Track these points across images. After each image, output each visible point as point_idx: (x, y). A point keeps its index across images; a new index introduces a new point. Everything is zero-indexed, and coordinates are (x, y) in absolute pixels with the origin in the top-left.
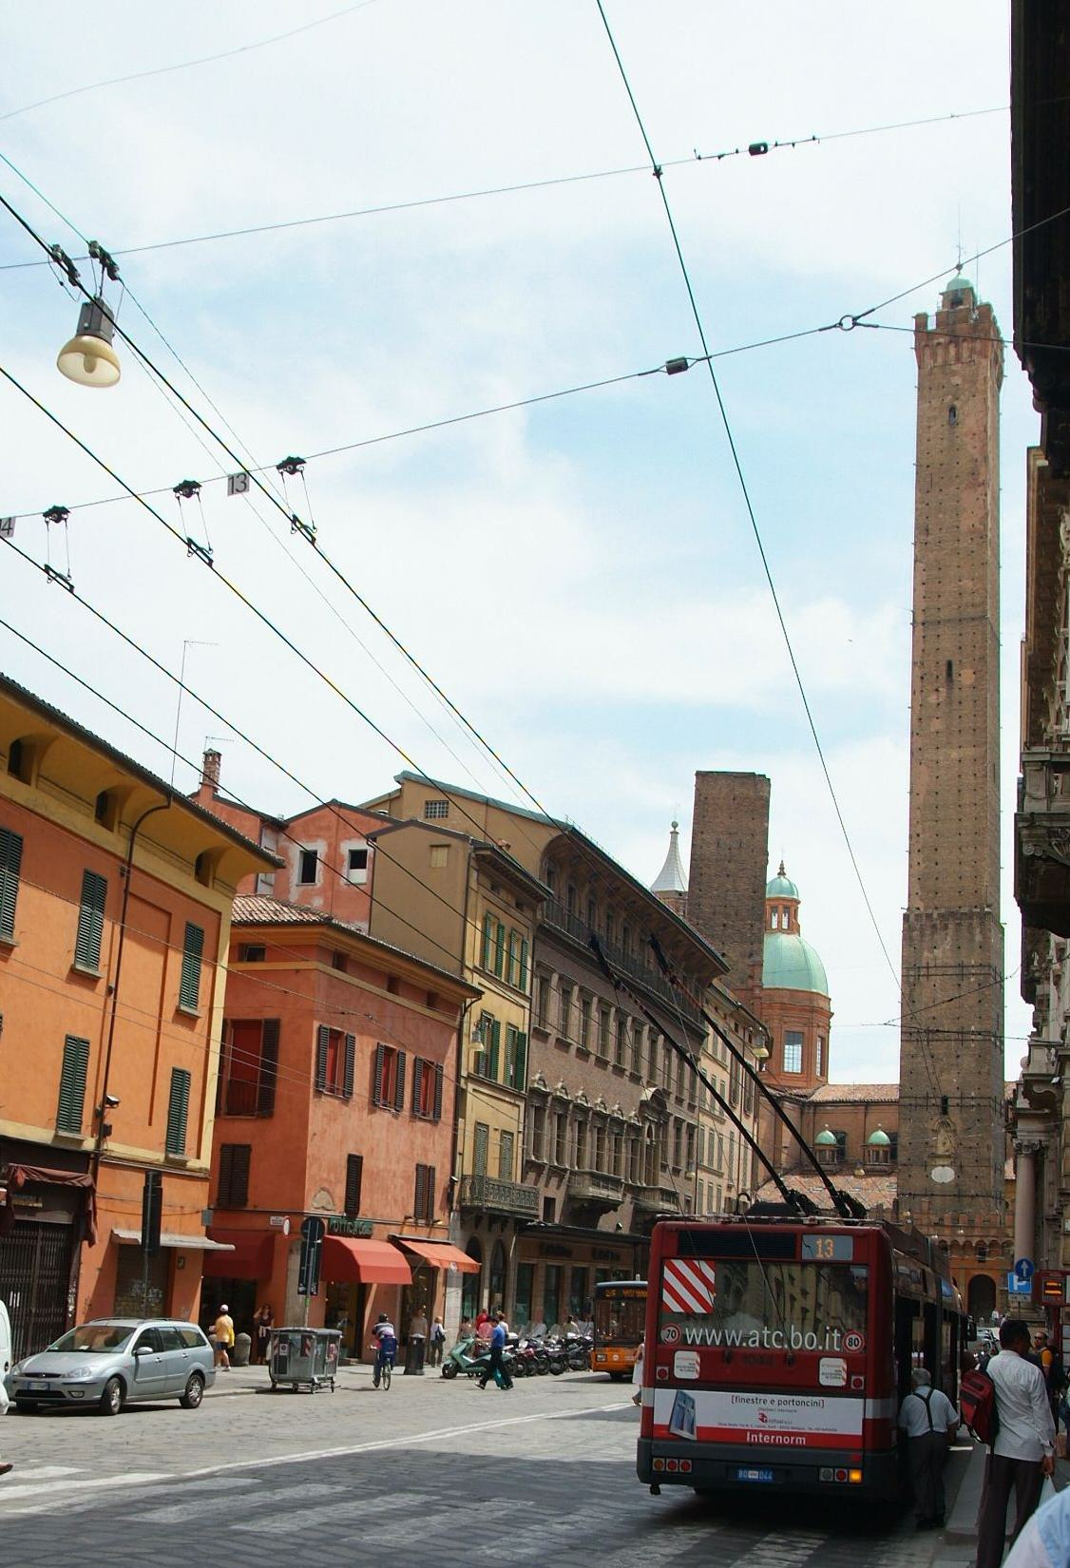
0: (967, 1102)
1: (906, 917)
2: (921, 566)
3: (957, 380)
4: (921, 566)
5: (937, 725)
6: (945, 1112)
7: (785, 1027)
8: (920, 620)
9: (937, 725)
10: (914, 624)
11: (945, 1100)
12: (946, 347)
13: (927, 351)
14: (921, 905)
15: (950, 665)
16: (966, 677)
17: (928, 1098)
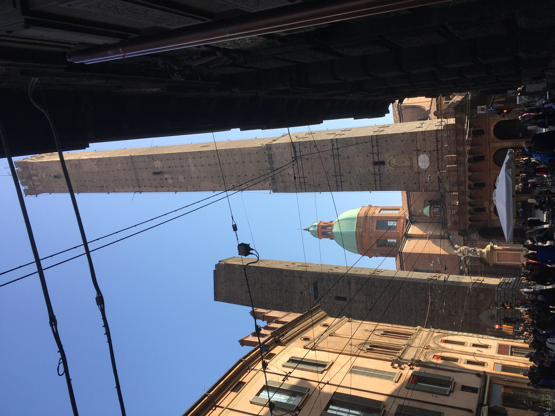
0: (375, 150)
1: (275, 191)
2: (116, 189)
3: (44, 175)
4: (116, 189)
5: (181, 178)
6: (383, 163)
7: (374, 230)
8: (137, 189)
9: (181, 178)
10: (141, 192)
11: (375, 163)
12: (33, 181)
13: (37, 189)
14: (268, 183)
15: (155, 173)
16: (158, 164)
17: (375, 174)
